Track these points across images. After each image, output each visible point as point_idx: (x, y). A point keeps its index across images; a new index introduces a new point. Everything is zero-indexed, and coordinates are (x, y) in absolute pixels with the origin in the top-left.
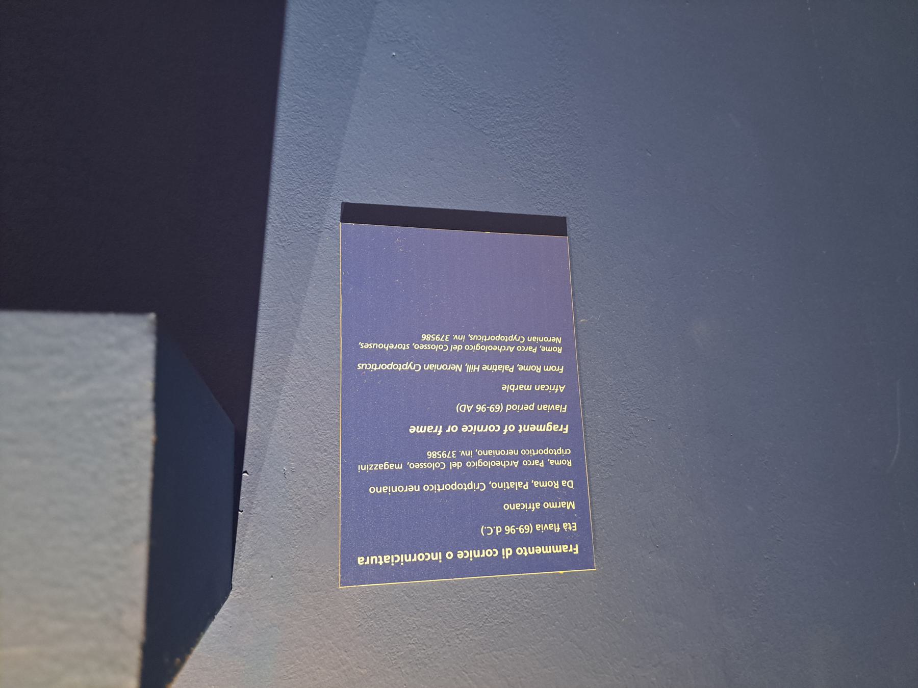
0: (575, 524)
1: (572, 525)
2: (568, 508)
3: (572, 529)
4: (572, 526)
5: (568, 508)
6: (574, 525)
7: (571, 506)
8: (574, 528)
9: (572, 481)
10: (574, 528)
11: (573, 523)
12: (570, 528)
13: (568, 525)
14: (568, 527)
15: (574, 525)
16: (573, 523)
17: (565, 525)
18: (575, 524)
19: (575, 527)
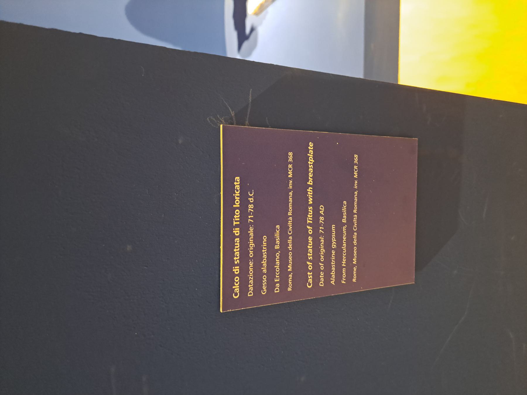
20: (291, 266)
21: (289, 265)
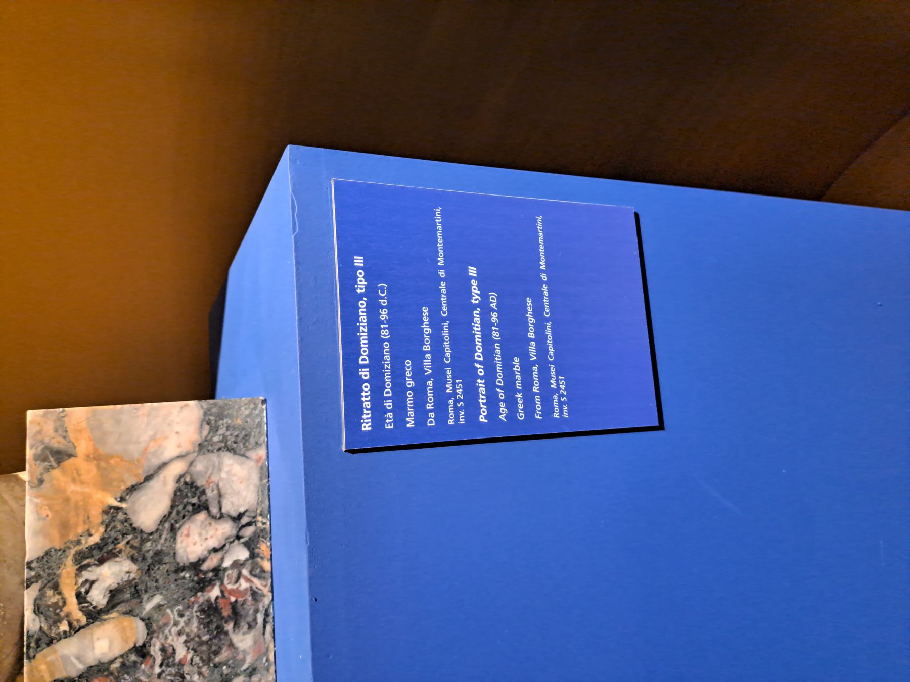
0: (392, 427)
1: (390, 423)
2: (408, 419)
4: (389, 423)
5: (408, 419)
6: (391, 426)
7: (410, 422)
8: (388, 426)
9: (434, 424)
10: (388, 426)
11: (392, 424)
12: (388, 421)
13: (391, 419)
14: (390, 419)
15: (391, 426)
16: (392, 424)
17: (390, 415)
18: (392, 427)
19: (389, 427)
20: (451, 385)
21: (447, 384)
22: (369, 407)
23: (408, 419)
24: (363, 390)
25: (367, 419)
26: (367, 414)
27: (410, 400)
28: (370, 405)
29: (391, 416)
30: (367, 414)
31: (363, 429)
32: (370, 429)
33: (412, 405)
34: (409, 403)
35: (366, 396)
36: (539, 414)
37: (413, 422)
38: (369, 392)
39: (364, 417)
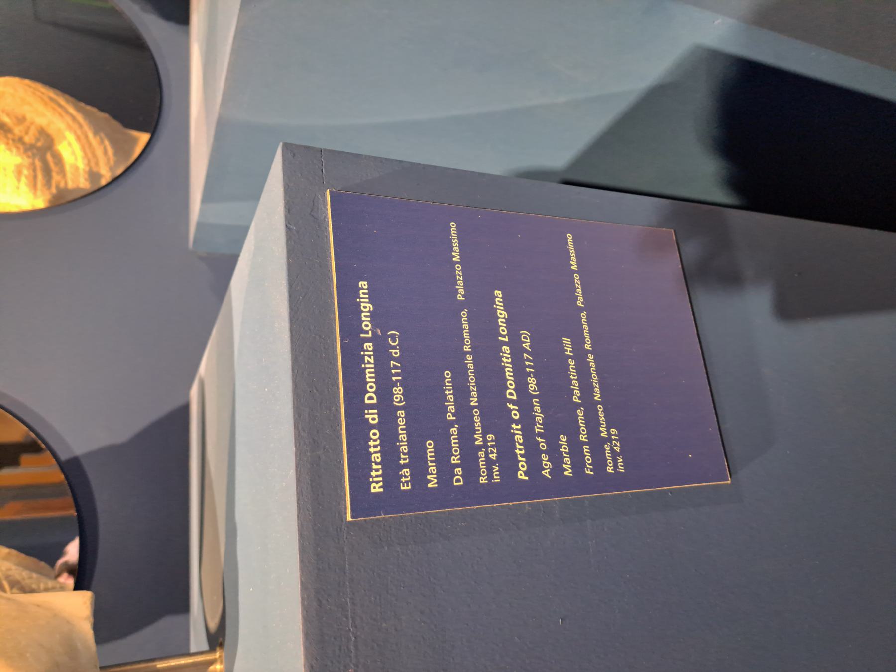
0: (409, 488)
1: (407, 482)
2: (429, 477)
3: (402, 482)
9: (462, 483)
11: (410, 483)
14: (406, 477)
15: (408, 486)
16: (410, 483)
17: (406, 471)
22: (379, 461)
23: (429, 477)
24: (371, 439)
25: (377, 476)
26: (377, 470)
27: (430, 452)
28: (380, 458)
29: (407, 472)
30: (377, 470)
31: (373, 490)
32: (381, 490)
33: (433, 459)
34: (430, 455)
35: (375, 446)
36: (590, 469)
37: (435, 481)
38: (379, 440)
39: (374, 474)
